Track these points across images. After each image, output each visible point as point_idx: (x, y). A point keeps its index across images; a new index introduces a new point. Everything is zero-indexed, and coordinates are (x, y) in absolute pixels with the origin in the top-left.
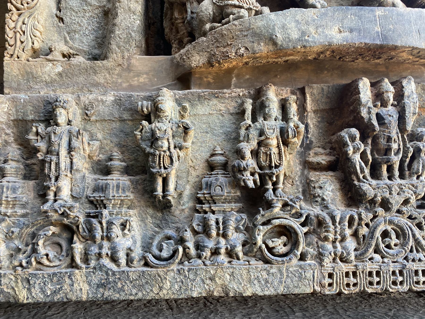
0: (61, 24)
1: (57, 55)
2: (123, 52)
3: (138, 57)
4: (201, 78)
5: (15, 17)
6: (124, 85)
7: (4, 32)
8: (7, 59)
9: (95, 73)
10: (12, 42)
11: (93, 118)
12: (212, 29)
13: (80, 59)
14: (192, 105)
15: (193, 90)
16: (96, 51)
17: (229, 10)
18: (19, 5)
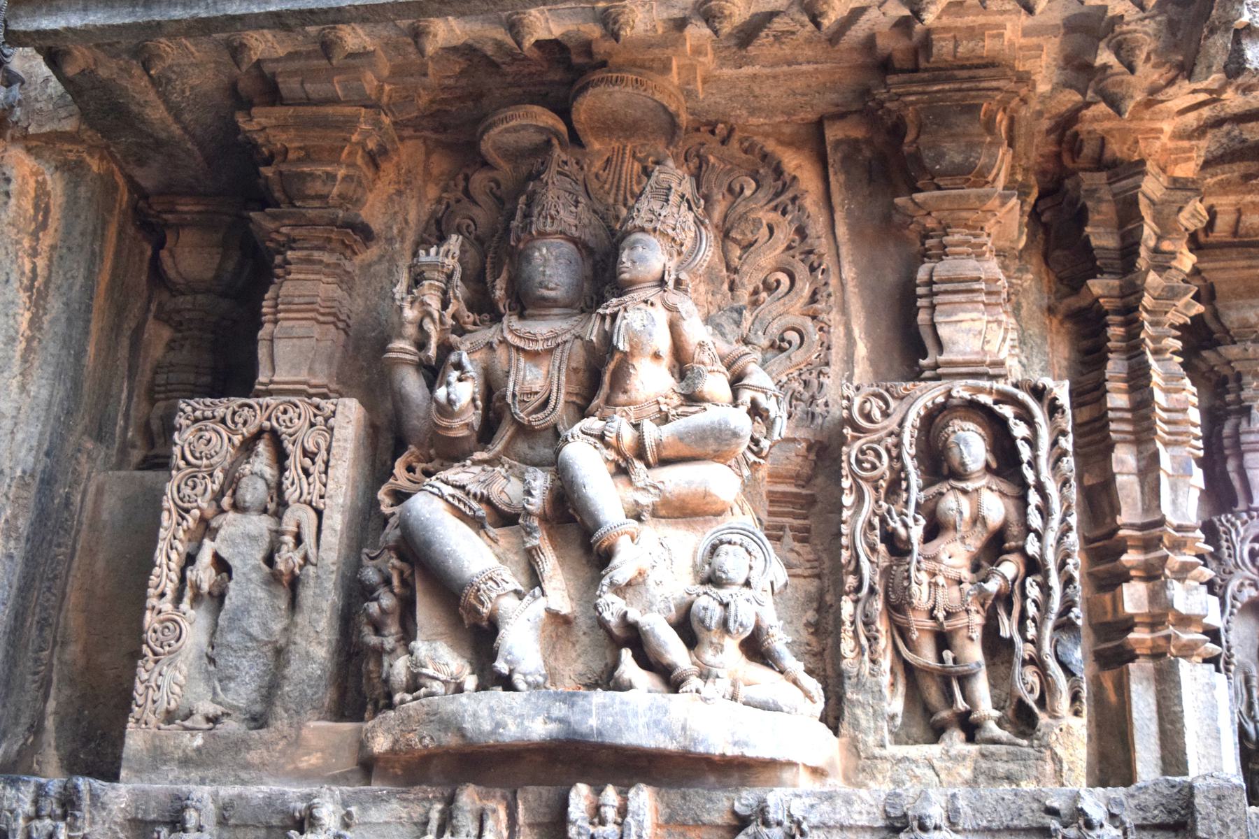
0: (212, 668)
1: (198, 721)
2: (291, 717)
3: (312, 724)
4: (386, 769)
5: (150, 665)
6: (290, 767)
7: (132, 688)
8: (131, 724)
9: (249, 748)
10: (140, 700)
11: (232, 821)
12: (403, 702)
13: (232, 726)
14: (364, 809)
15: (375, 787)
16: (258, 708)
17: (422, 681)
18: (159, 649)
